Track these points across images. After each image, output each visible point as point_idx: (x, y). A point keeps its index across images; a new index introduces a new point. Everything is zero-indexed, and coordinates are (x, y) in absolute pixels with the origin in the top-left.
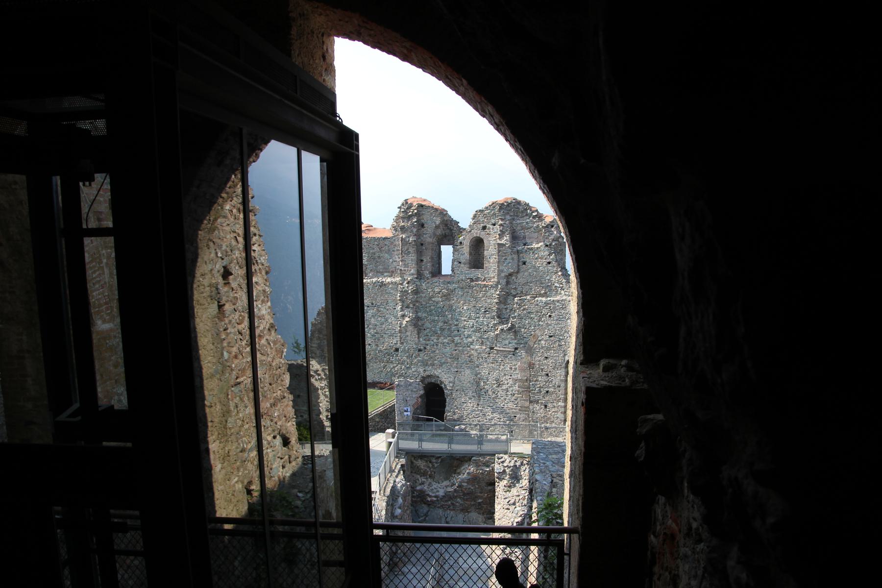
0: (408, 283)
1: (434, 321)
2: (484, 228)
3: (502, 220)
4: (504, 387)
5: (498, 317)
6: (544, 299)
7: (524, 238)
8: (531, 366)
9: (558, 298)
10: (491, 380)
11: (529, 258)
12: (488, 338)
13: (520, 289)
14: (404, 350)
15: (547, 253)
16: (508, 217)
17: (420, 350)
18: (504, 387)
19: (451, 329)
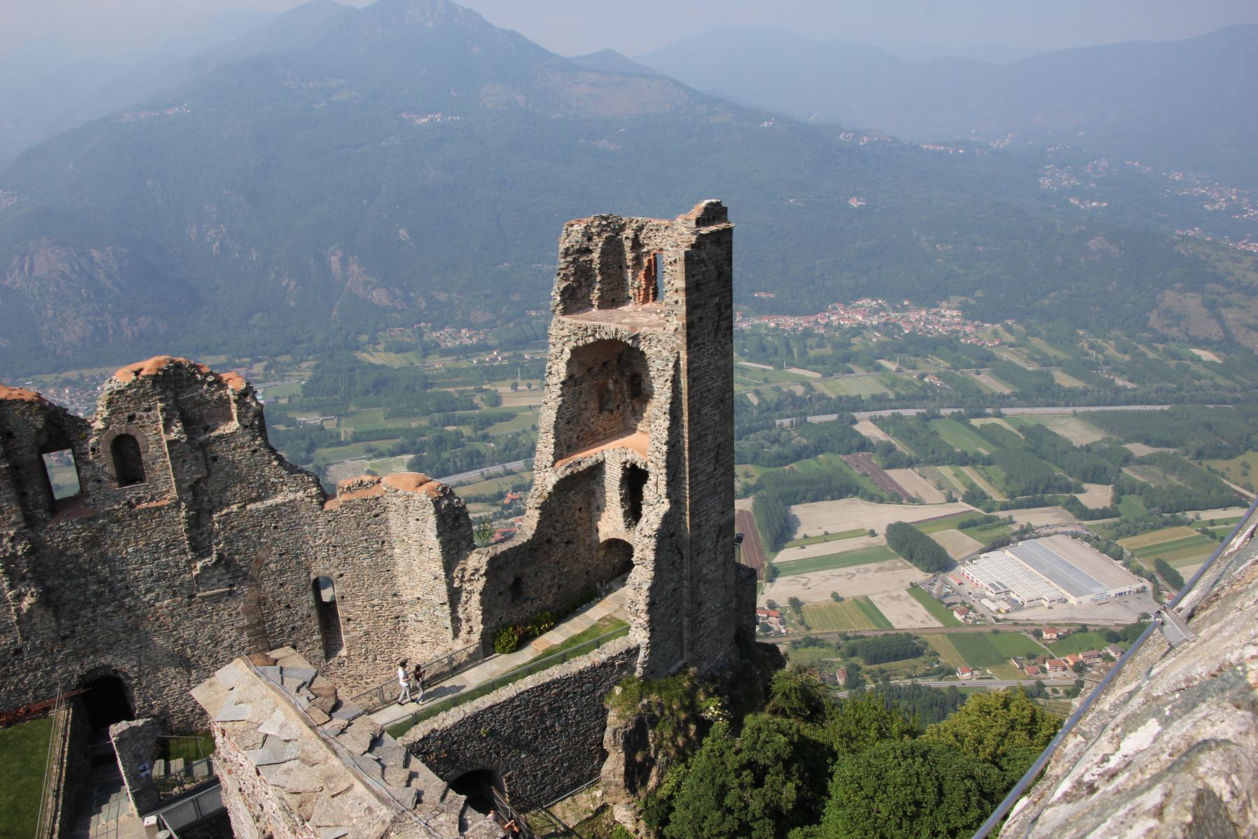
0: (12, 540)
1: (78, 586)
2: (131, 418)
3: (161, 400)
4: (226, 644)
5: (194, 549)
6: (259, 505)
7: (202, 419)
8: (261, 602)
9: (279, 499)
10: (203, 639)
11: (220, 449)
12: (182, 584)
13: (216, 499)
14: (35, 649)
15: (248, 437)
16: (169, 393)
17: (64, 638)
18: (226, 644)
19: (115, 590)
